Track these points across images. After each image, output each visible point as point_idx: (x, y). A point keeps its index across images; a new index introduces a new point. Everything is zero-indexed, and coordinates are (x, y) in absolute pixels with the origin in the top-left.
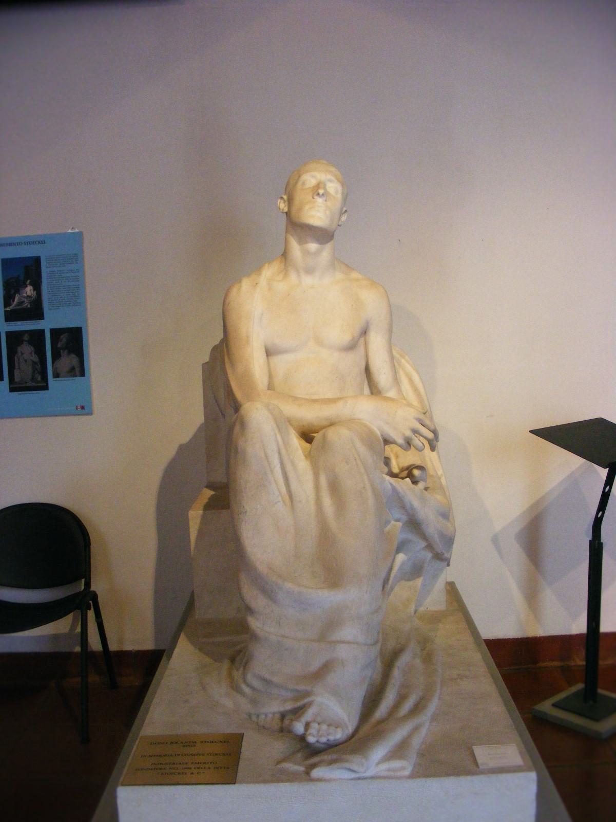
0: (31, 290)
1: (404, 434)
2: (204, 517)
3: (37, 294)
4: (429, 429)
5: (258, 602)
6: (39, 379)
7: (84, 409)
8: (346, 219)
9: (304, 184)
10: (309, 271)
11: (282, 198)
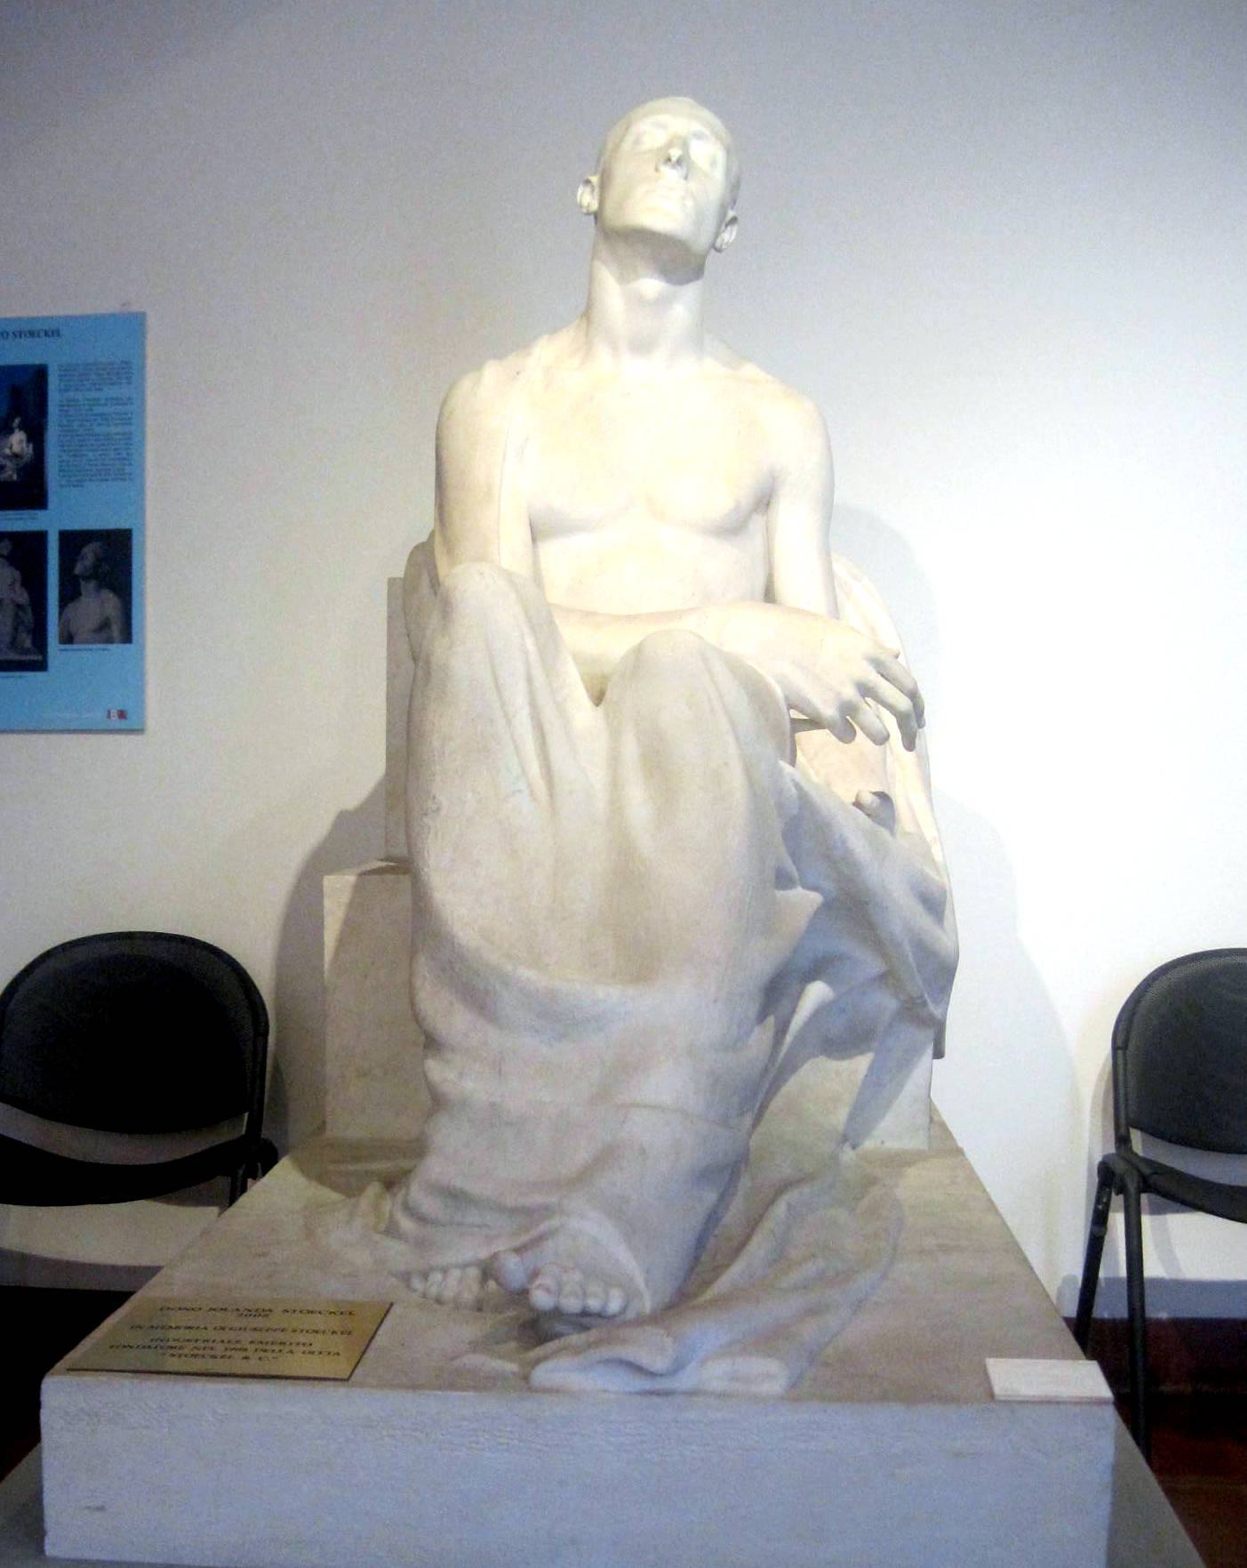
0: (21, 441)
1: (838, 694)
2: (358, 889)
3: (34, 449)
4: (901, 690)
5: (453, 1020)
6: (28, 643)
7: (126, 720)
8: (736, 239)
9: (637, 142)
10: (642, 345)
11: (588, 182)
